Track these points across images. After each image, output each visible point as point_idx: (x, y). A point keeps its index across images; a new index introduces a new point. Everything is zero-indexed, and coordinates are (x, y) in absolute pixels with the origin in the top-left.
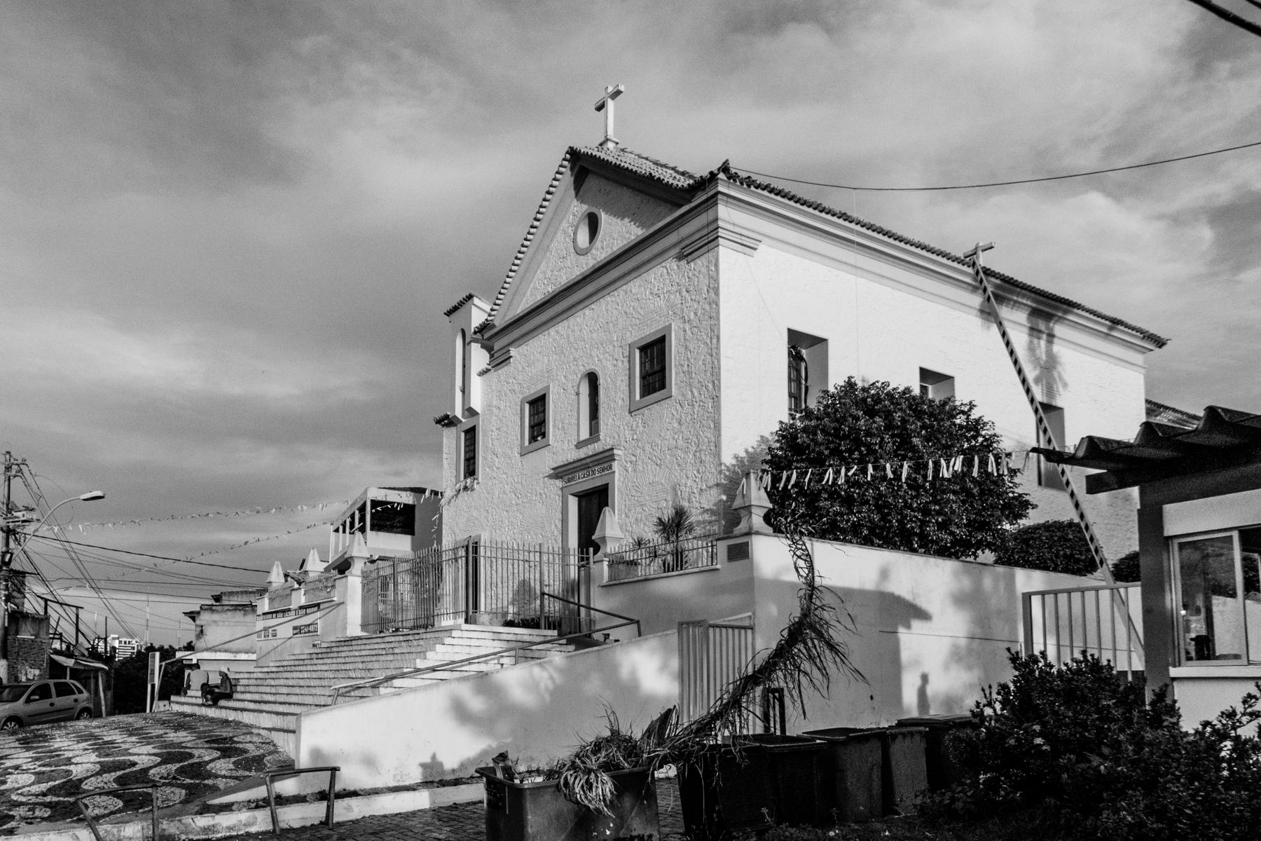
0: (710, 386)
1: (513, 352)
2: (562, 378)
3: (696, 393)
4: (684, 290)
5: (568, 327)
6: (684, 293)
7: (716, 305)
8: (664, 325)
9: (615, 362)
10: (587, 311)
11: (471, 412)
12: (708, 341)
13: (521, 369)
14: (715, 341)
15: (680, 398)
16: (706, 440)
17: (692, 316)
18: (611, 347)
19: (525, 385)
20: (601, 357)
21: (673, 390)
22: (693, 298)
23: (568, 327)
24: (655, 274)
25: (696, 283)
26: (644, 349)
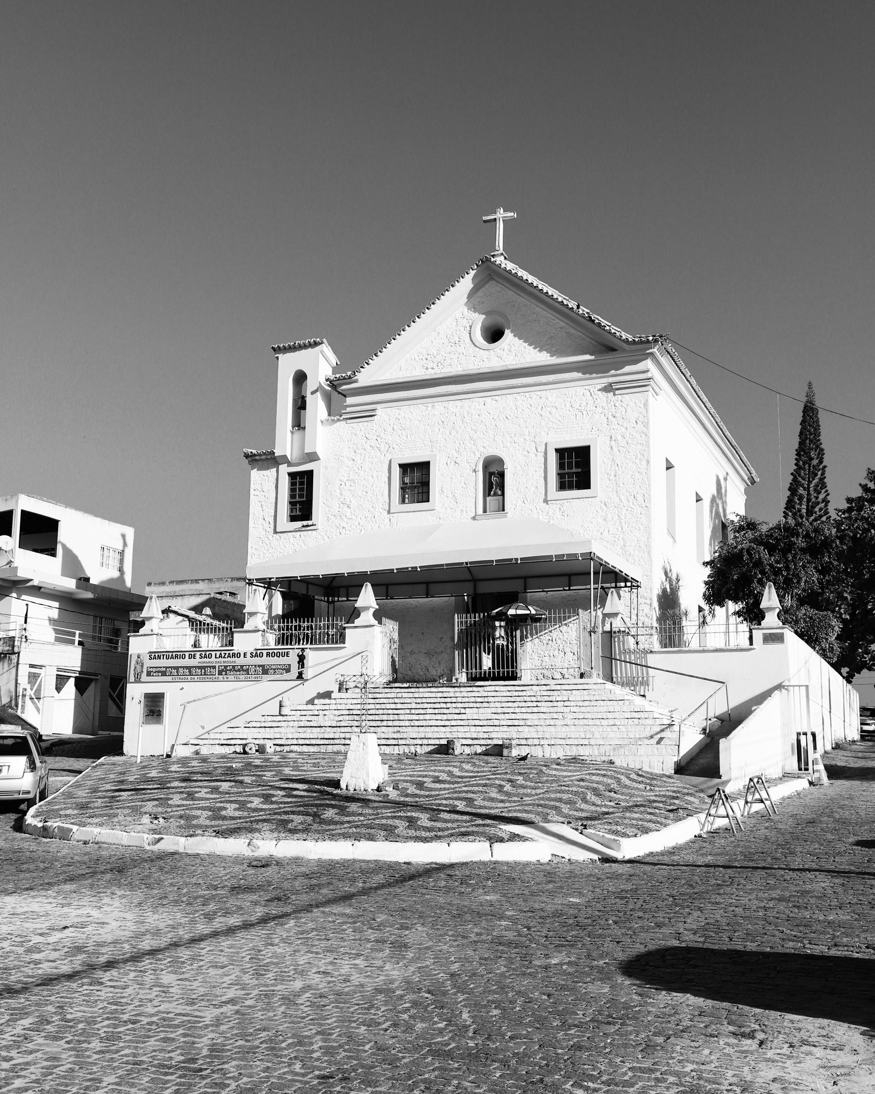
0: (640, 498)
1: (381, 411)
2: (454, 452)
3: (623, 498)
4: (610, 414)
5: (462, 407)
6: (610, 417)
7: (646, 435)
8: (587, 437)
9: (526, 453)
10: (488, 400)
11: (313, 457)
12: (637, 461)
13: (390, 430)
14: (644, 463)
15: (606, 500)
16: (636, 539)
17: (619, 438)
18: (522, 440)
19: (396, 447)
20: (509, 444)
21: (599, 492)
22: (620, 423)
23: (462, 407)
24: (576, 392)
25: (624, 413)
26: (562, 453)
